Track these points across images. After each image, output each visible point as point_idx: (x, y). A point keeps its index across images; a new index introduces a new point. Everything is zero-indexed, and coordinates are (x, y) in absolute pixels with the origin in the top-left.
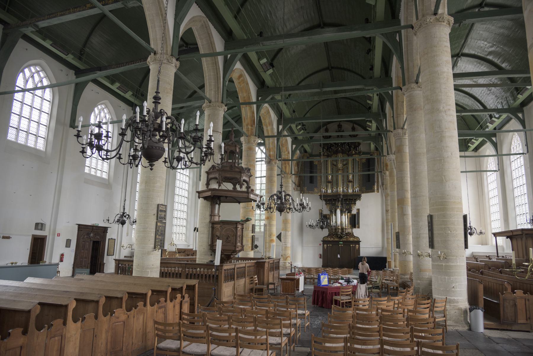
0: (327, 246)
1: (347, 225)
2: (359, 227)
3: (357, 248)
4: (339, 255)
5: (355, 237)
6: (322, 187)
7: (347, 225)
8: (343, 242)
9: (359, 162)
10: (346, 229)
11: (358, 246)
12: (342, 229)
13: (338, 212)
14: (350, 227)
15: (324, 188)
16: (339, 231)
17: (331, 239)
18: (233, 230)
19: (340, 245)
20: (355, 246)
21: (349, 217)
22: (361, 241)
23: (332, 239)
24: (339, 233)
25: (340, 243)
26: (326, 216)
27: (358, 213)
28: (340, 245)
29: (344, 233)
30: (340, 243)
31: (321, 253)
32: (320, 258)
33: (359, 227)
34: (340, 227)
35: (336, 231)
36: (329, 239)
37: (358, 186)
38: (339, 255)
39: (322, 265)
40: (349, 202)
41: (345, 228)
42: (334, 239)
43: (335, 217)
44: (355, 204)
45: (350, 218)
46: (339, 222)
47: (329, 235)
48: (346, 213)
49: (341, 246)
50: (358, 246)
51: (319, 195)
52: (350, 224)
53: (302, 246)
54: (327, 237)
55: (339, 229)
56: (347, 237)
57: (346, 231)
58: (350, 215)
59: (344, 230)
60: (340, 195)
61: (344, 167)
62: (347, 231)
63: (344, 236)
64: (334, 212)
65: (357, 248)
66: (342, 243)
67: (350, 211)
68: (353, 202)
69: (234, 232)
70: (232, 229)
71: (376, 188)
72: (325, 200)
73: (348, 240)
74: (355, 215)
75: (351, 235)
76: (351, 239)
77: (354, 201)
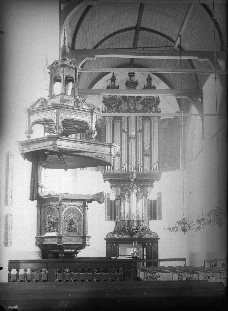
2: (161, 220)
5: (151, 233)
12: (138, 222)
13: (133, 197)
18: (78, 211)
22: (160, 239)
23: (120, 236)
27: (160, 198)
29: (141, 227)
33: (161, 220)
34: (135, 219)
36: (116, 236)
43: (128, 204)
44: (152, 186)
46: (134, 212)
54: (113, 233)
55: (134, 221)
57: (143, 225)
60: (133, 173)
64: (126, 198)
67: (145, 195)
68: (149, 184)
69: (80, 214)
70: (76, 209)
72: (111, 181)
74: (155, 201)
75: (146, 230)
76: (147, 236)
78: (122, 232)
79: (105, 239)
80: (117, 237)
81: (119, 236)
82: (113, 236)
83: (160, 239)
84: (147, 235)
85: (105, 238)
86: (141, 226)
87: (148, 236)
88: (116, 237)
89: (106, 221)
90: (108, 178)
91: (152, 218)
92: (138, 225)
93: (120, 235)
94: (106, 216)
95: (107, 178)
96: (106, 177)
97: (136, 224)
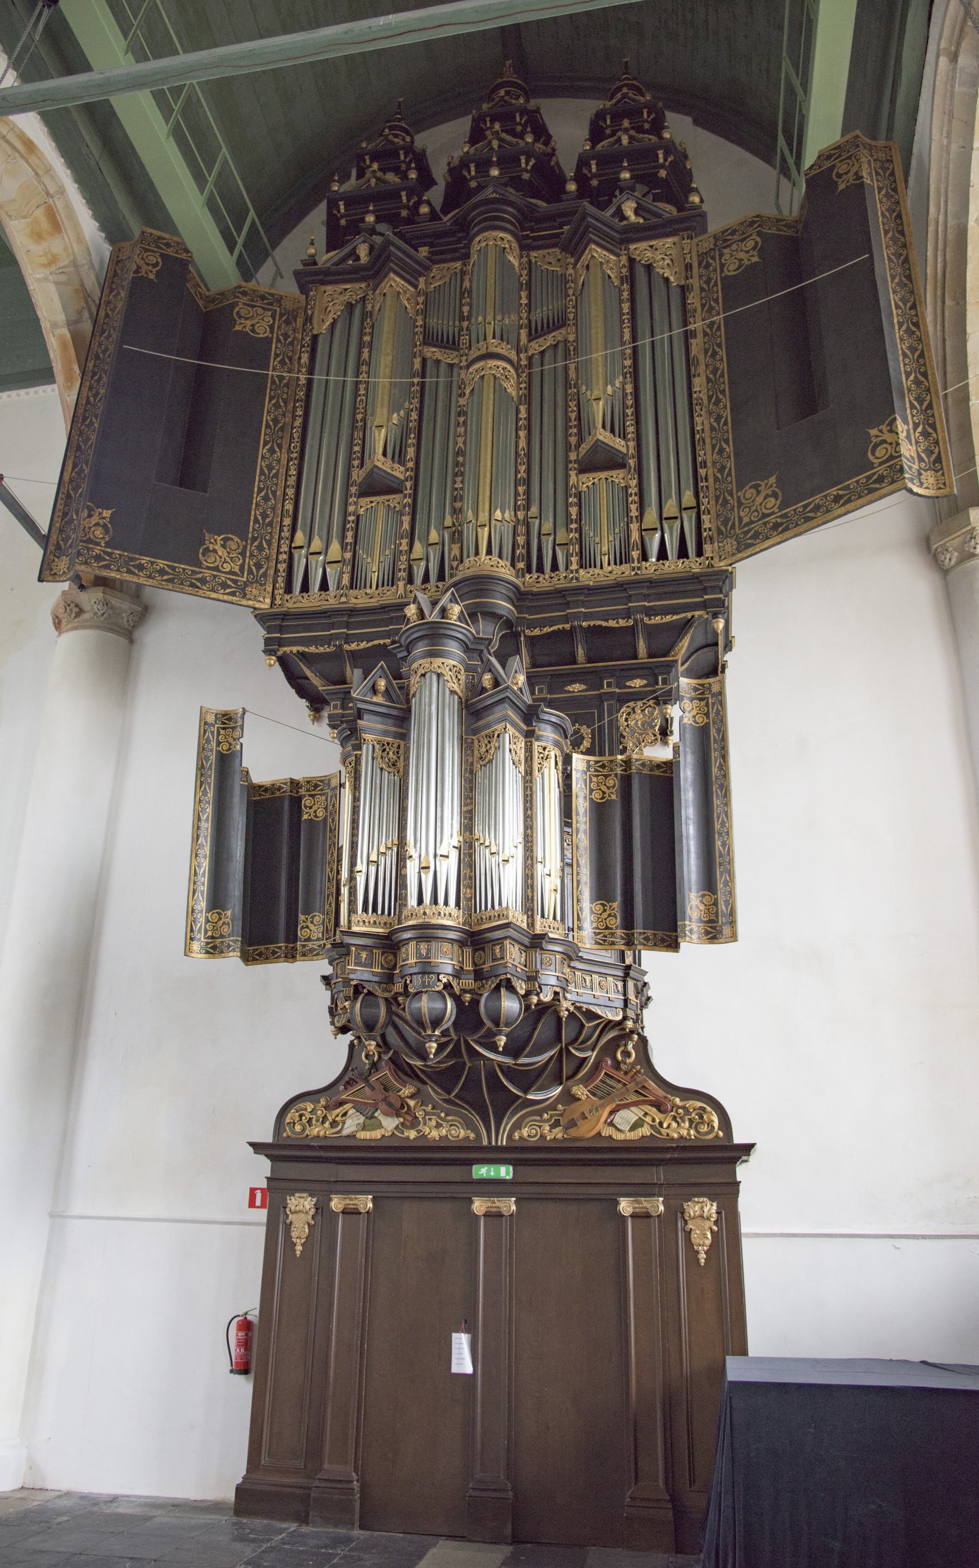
0: (321, 1209)
1: (551, 900)
3: (702, 1239)
4: (461, 1343)
6: (300, 538)
7: (551, 900)
8: (515, 1163)
9: (684, 290)
10: (536, 942)
11: (711, 1208)
14: (604, 939)
15: (317, 544)
16: (427, 969)
17: (371, 1122)
19: (479, 1206)
20: (676, 1213)
21: (581, 805)
22: (747, 1149)
23: (389, 1124)
24: (425, 1005)
25: (482, 1172)
26: (296, 802)
28: (479, 1206)
30: (482, 1172)
31: (251, 1304)
32: (243, 1368)
35: (389, 979)
36: (352, 1124)
37: (688, 498)
38: (461, 1343)
39: (238, 1469)
40: (592, 678)
41: (521, 920)
42: (414, 1123)
45: (599, 811)
47: (347, 1079)
48: (548, 733)
49: (494, 1216)
50: (711, 1208)
51: (262, 618)
52: (602, 892)
53: (57, 1216)
55: (427, 932)
56: (569, 1098)
57: (532, 978)
58: (601, 771)
59: (514, 956)
61: (536, 347)
62: (549, 978)
63: (528, 1080)
65: (702, 1239)
66: (505, 1172)
68: (637, 683)
71: (908, 450)
73: (585, 1131)
77: (651, 673)
78: (406, 1091)
79: (257, 1147)
80: (362, 1135)
81: (380, 1126)
82: (334, 1124)
83: (747, 1149)
84: (626, 1118)
85: (268, 1138)
86: (511, 989)
87: (634, 1127)
88: (352, 1136)
89: (187, 952)
90: (301, 649)
91: (637, 931)
92: (479, 975)
93: (386, 1114)
94: (191, 911)
95: (295, 649)
96: (281, 643)
97: (458, 974)
